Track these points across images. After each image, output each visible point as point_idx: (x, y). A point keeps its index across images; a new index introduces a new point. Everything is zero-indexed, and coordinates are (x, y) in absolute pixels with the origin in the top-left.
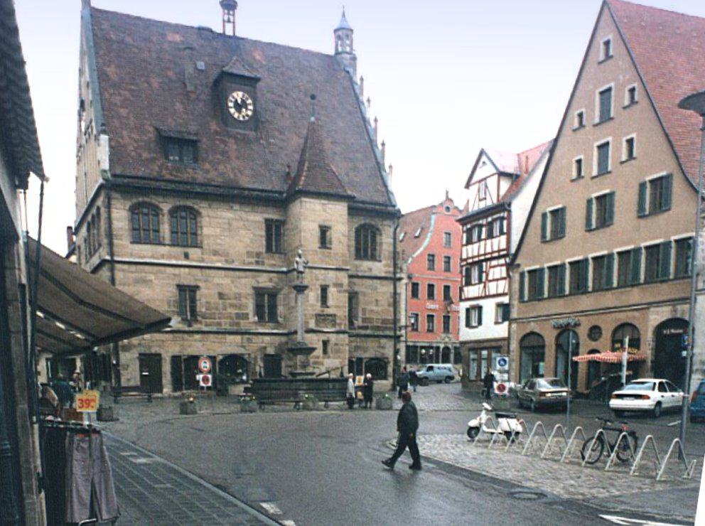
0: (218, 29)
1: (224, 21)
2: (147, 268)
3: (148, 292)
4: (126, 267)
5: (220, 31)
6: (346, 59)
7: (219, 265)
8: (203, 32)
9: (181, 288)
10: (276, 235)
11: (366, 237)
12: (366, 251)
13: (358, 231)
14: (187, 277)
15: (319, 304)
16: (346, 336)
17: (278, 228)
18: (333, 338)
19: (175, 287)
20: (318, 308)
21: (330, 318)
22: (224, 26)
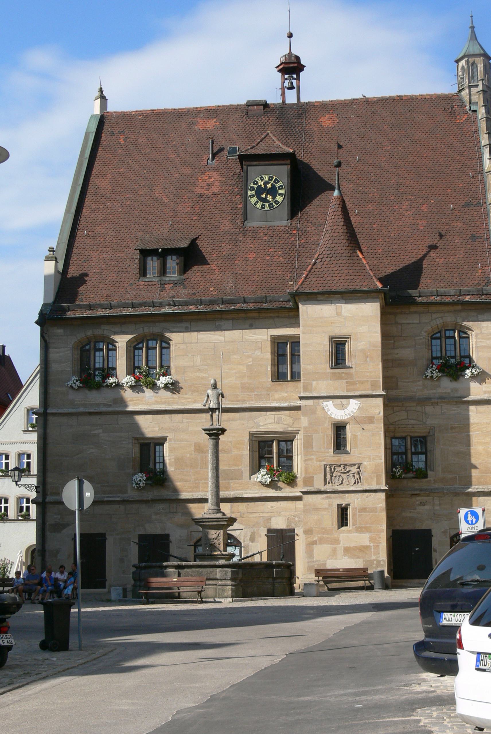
0: (274, 99)
1: (283, 89)
2: (95, 419)
4: (64, 420)
15: (331, 451)
18: (355, 501)
20: (329, 456)
22: (283, 94)
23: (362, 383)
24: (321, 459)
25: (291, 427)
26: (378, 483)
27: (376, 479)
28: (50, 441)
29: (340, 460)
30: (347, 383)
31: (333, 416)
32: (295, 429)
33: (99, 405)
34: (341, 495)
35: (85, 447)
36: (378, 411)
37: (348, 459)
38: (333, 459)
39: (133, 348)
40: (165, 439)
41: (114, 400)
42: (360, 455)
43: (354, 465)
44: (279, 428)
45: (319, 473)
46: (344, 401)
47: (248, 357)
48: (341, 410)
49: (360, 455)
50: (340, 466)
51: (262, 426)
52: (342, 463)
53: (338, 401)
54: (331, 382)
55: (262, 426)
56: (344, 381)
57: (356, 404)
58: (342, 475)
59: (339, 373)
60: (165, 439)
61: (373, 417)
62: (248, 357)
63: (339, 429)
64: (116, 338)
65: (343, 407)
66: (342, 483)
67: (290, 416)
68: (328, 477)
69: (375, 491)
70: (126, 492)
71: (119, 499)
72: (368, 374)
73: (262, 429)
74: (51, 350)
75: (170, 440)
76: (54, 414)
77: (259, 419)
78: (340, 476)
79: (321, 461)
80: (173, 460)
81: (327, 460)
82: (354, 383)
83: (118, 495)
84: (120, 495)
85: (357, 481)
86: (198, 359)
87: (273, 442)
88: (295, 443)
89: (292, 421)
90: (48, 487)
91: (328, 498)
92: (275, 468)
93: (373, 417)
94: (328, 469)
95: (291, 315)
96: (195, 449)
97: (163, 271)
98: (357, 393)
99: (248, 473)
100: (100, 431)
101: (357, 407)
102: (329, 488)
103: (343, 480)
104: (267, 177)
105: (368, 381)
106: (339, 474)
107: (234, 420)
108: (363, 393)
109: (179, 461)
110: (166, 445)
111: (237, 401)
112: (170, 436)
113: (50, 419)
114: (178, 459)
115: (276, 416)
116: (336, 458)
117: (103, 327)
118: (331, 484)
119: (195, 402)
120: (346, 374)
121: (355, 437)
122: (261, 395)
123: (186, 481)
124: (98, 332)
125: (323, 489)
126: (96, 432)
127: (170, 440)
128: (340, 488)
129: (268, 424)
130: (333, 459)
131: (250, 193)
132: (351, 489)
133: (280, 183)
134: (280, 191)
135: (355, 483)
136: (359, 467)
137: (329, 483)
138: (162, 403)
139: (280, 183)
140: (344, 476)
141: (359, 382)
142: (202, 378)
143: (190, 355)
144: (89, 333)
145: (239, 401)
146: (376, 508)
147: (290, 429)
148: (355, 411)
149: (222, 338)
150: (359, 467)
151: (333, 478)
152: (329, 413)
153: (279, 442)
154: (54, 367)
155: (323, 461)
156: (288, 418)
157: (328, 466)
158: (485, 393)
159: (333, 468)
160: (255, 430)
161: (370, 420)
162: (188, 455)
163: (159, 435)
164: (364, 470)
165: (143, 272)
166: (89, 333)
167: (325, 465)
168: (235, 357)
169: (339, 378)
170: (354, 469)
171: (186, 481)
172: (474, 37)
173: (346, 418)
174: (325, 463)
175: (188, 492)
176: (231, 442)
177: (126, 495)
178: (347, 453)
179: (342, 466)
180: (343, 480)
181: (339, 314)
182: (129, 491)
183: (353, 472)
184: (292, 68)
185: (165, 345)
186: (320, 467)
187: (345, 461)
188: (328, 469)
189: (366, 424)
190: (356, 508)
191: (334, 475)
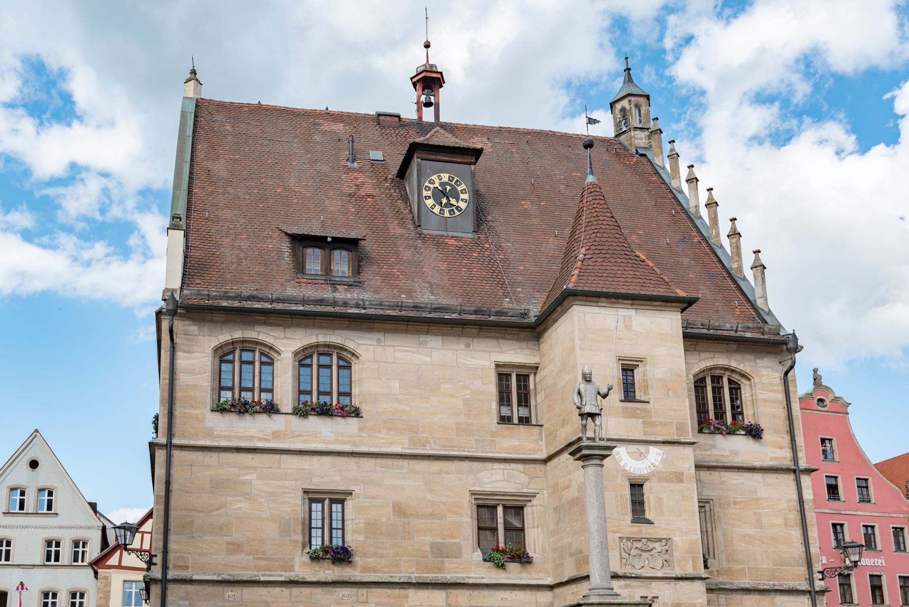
3: (240, 505)
5: (414, 116)
6: (641, 139)
7: (398, 449)
8: (386, 122)
9: (312, 497)
10: (515, 391)
11: (717, 390)
12: (720, 415)
13: (699, 385)
14: (326, 475)
15: (629, 517)
16: (700, 586)
17: (523, 379)
19: (300, 494)
21: (657, 546)
23: (665, 425)
25: (526, 488)
26: (694, 568)
27: (691, 562)
28: (174, 487)
29: (640, 531)
30: (644, 423)
31: (627, 468)
32: (532, 491)
33: (251, 438)
34: (647, 582)
35: (229, 499)
36: (688, 466)
37: (651, 531)
38: (631, 529)
39: (303, 358)
40: (350, 493)
41: (274, 433)
43: (660, 540)
44: (510, 488)
46: (642, 448)
47: (465, 387)
48: (638, 460)
51: (488, 483)
53: (633, 448)
54: (622, 420)
55: (488, 483)
56: (640, 421)
57: (657, 454)
58: (643, 553)
59: (632, 409)
60: (350, 493)
61: (682, 474)
62: (465, 387)
63: (636, 487)
64: (279, 345)
65: (641, 456)
67: (524, 472)
69: (693, 579)
70: (291, 569)
71: (282, 579)
72: (672, 413)
73: (488, 488)
74: (179, 355)
75: (358, 496)
76: (182, 447)
77: (483, 473)
80: (362, 525)
82: (653, 424)
83: (281, 573)
84: (283, 573)
86: (396, 385)
87: (495, 507)
88: (527, 510)
89: (527, 480)
90: (171, 556)
91: (626, 586)
92: (502, 545)
93: (682, 474)
95: (534, 330)
96: (394, 511)
97: (327, 270)
98: (660, 439)
99: (470, 549)
100: (254, 476)
101: (659, 458)
102: (627, 570)
104: (447, 176)
105: (672, 423)
107: (448, 473)
108: (670, 438)
109: (371, 528)
110: (349, 504)
111: (450, 446)
112: (357, 489)
113: (176, 453)
114: (369, 524)
115: (506, 471)
116: (635, 529)
117: (258, 328)
119: (391, 444)
120: (642, 410)
121: (660, 499)
122: (483, 440)
123: (382, 556)
124: (251, 334)
126: (247, 477)
127: (358, 496)
129: (498, 481)
130: (631, 529)
131: (425, 193)
133: (463, 186)
134: (463, 196)
138: (345, 443)
139: (463, 186)
141: (661, 423)
142: (403, 412)
143: (384, 379)
144: (238, 334)
145: (454, 447)
146: (694, 605)
147: (525, 491)
148: (657, 464)
149: (428, 359)
152: (622, 464)
153: (505, 508)
154: (182, 379)
155: (617, 532)
156: (522, 475)
158: (772, 459)
160: (478, 489)
161: (679, 477)
162: (384, 519)
163: (342, 487)
165: (299, 266)
166: (238, 334)
168: (447, 386)
169: (632, 415)
171: (382, 556)
172: (629, 80)
173: (646, 472)
174: (620, 535)
175: (385, 573)
176: (444, 503)
177: (292, 574)
178: (649, 522)
181: (628, 328)
182: (297, 568)
184: (429, 82)
185: (348, 361)
187: (647, 534)
189: (672, 482)
190: (667, 604)
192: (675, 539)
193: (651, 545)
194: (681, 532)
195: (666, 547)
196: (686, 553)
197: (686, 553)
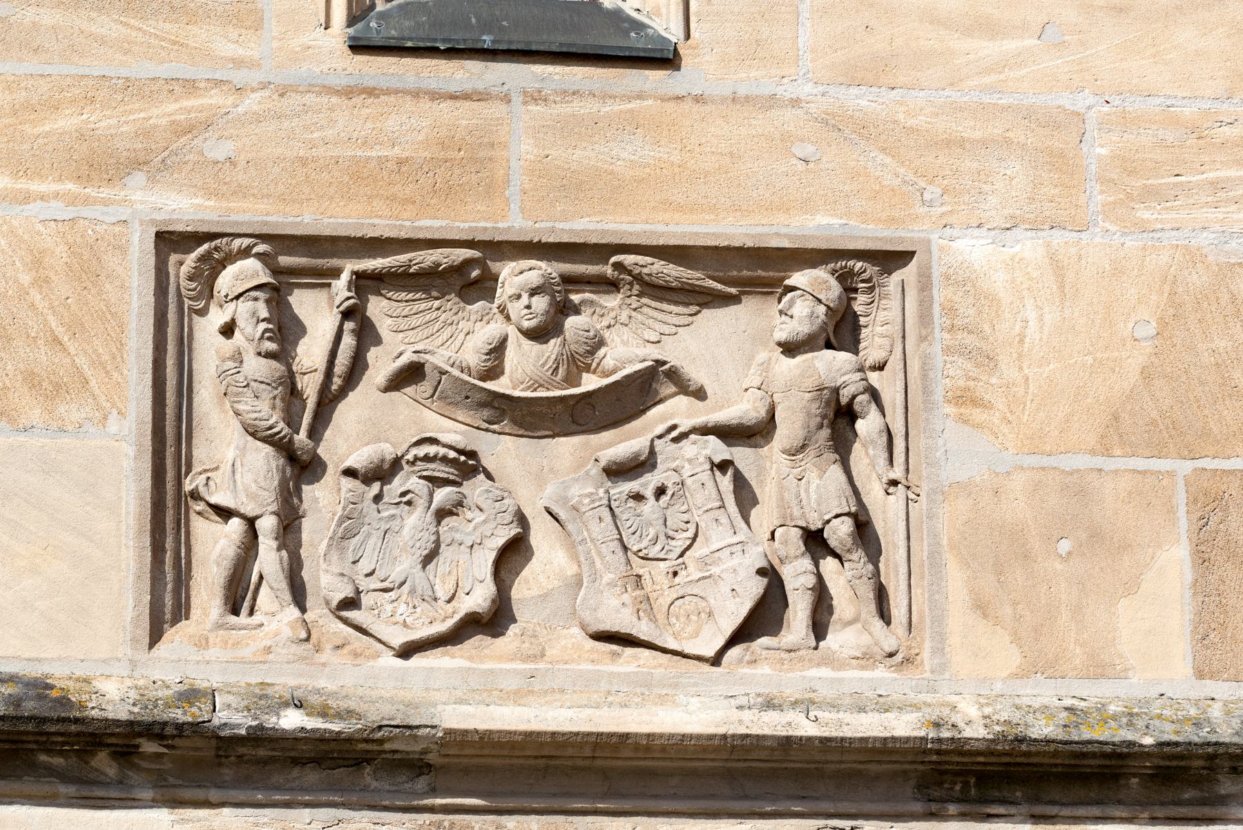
24: (115, 123)
27: (1175, 559)
37: (628, 153)
38: (346, 129)
42: (860, 100)
43: (750, 272)
45: (51, 389)
49: (860, 100)
50: (468, 280)
52: (515, 222)
58: (503, 451)
66: (493, 621)
68: (235, 466)
78: (467, 465)
79: (104, 165)
81: (219, 150)
85: (797, 576)
94: (227, 349)
102: (238, 666)
103: (513, 554)
106: (453, 431)
118: (273, 609)
125: (114, 675)
128: (468, 696)
130: (346, 129)
132: (696, 708)
135: (763, 619)
136: (841, 330)
137: (238, 594)
140: (542, 474)
150: (841, 330)
151: (323, 500)
157: (244, 272)
159: (319, 313)
164: (951, 373)
167: (169, 241)
170: (736, 357)
179: (515, 276)
180: (513, 554)
183: (744, 409)
186: (88, 268)
187: (573, 185)
188: (227, 349)
191: (354, 435)
192: (970, 251)
193: (627, 338)
194: (1062, 165)
195: (832, 365)
196: (1115, 433)
197: (1115, 433)
